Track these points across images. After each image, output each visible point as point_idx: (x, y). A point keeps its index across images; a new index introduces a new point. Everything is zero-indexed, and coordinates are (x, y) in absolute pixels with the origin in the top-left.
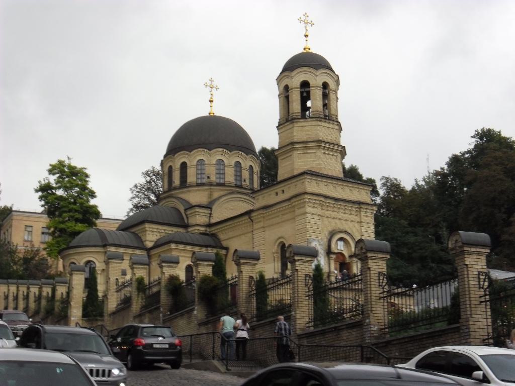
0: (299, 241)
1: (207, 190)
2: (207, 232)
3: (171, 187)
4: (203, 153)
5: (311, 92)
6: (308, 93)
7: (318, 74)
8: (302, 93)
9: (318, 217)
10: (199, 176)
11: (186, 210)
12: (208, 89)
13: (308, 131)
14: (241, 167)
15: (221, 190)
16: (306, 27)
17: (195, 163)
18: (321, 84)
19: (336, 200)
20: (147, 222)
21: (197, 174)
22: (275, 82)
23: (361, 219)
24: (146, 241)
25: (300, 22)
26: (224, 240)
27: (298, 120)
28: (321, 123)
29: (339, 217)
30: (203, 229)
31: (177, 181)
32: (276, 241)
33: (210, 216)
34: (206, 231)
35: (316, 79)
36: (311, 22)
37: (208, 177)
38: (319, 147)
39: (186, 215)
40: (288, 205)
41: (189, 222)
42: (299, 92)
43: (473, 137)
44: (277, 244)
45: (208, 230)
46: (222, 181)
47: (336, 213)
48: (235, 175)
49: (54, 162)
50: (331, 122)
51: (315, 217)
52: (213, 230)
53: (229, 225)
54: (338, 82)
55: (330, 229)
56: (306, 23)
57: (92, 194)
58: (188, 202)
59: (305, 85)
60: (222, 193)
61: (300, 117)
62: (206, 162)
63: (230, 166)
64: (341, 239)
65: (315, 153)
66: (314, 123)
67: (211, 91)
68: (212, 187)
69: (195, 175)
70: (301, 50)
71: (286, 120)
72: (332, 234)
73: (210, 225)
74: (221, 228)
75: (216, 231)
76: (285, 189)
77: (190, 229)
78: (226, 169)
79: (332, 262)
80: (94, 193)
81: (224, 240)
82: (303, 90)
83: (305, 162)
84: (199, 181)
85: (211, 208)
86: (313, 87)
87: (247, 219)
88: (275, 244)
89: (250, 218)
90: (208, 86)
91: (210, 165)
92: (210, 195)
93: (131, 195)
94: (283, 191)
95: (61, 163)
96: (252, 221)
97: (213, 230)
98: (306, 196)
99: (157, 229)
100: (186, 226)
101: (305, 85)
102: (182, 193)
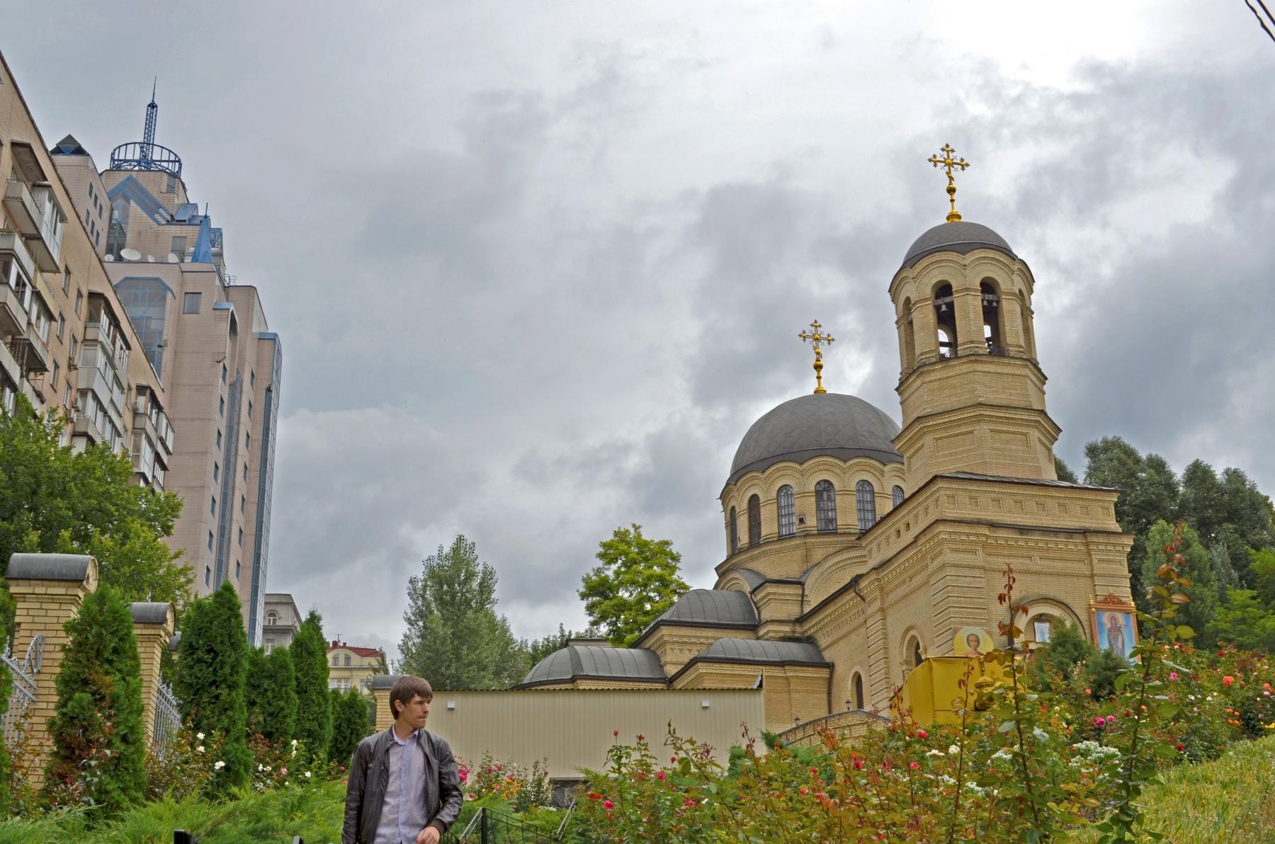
1: (798, 547)
3: (734, 551)
4: (789, 472)
7: (967, 262)
8: (938, 308)
9: (977, 573)
10: (784, 521)
13: (955, 387)
14: (872, 492)
15: (824, 544)
17: (774, 494)
19: (1022, 530)
22: (888, 296)
23: (1092, 569)
24: (666, 663)
27: (931, 368)
28: (979, 367)
29: (1033, 568)
30: (786, 629)
31: (744, 538)
34: (794, 632)
37: (801, 521)
38: (979, 419)
45: (798, 629)
47: (1028, 561)
48: (859, 510)
50: (1006, 361)
51: (967, 572)
52: (809, 628)
53: (833, 612)
54: (1029, 279)
56: (950, 165)
58: (758, 574)
59: (944, 290)
60: (831, 550)
62: (795, 490)
63: (845, 492)
64: (1040, 618)
65: (971, 432)
66: (965, 368)
67: (815, 348)
68: (809, 540)
71: (912, 371)
74: (819, 622)
76: (910, 518)
77: (761, 632)
82: (940, 301)
83: (950, 455)
84: (785, 531)
85: (802, 584)
86: (958, 291)
87: (852, 599)
88: (902, 643)
91: (803, 494)
92: (807, 558)
95: (621, 536)
98: (941, 528)
100: (752, 627)
101: (944, 290)
102: (752, 559)
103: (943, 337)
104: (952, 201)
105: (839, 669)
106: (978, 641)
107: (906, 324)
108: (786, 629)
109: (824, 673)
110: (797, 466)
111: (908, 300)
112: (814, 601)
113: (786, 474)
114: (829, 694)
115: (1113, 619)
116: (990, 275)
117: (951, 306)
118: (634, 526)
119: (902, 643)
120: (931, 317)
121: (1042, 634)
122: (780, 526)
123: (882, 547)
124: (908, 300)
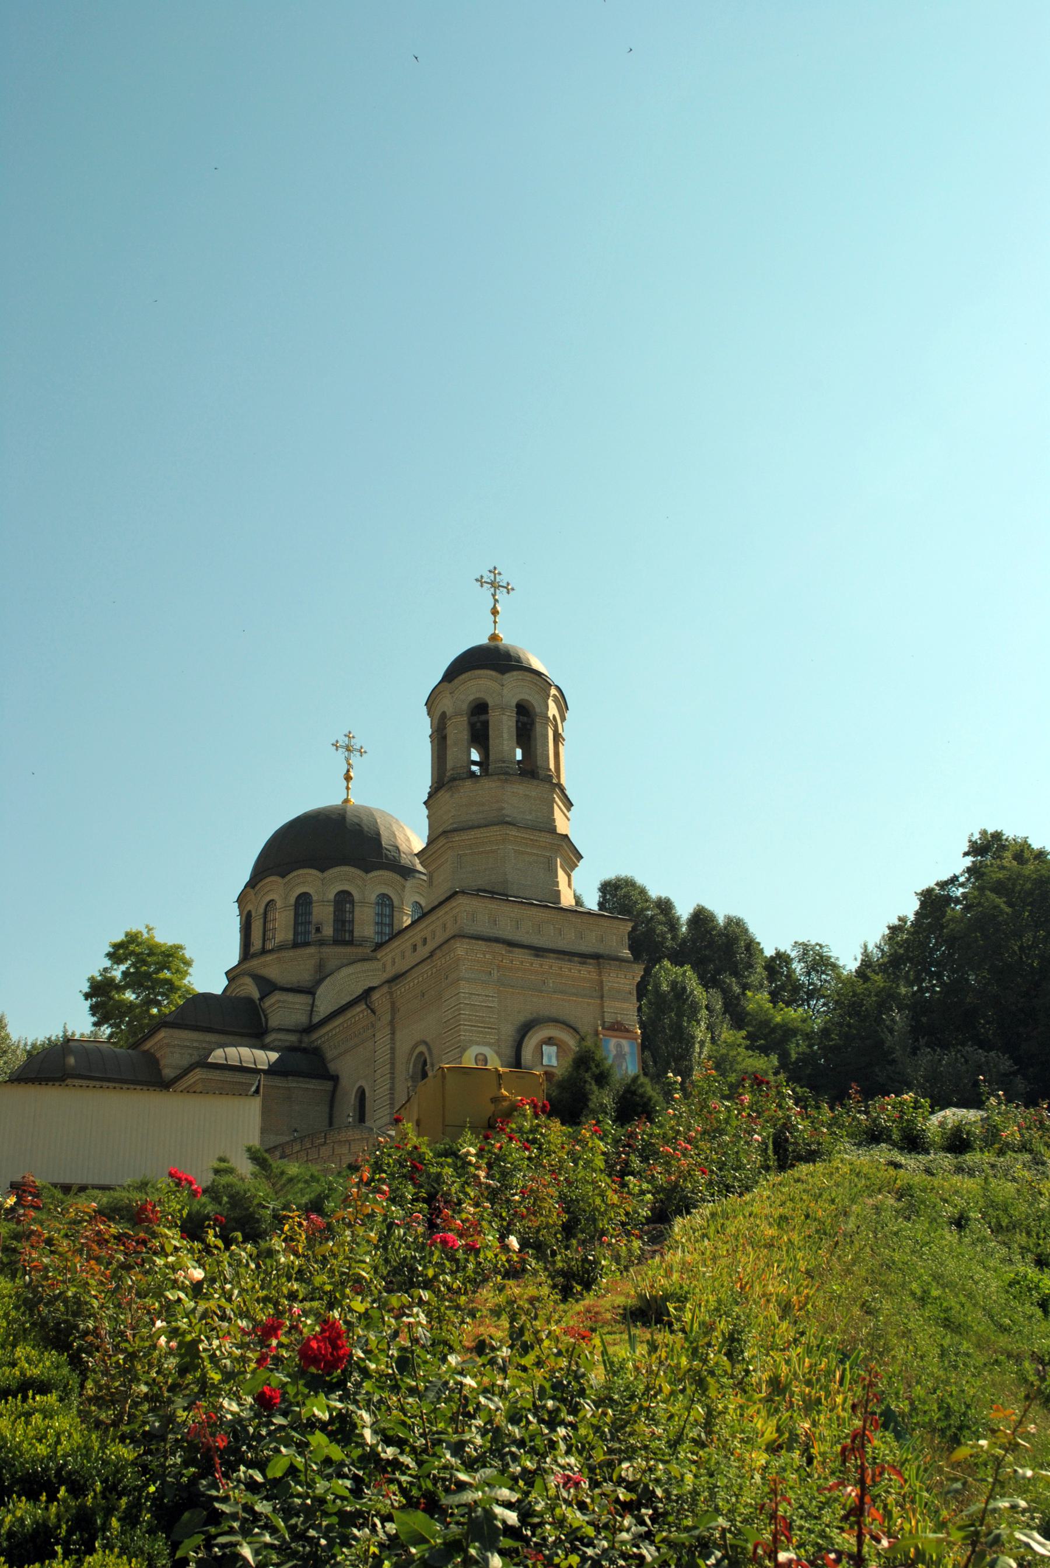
0: (448, 1047)
8: (472, 726)
12: (342, 753)
14: (392, 906)
16: (494, 595)
17: (292, 900)
18: (514, 703)
19: (539, 951)
20: (165, 1027)
21: (296, 924)
33: (312, 1011)
34: (300, 1042)
35: (505, 692)
37: (318, 930)
42: (466, 723)
43: (966, 854)
49: (120, 937)
55: (522, 1018)
64: (550, 1041)
67: (347, 760)
70: (484, 640)
72: (525, 1029)
78: (357, 909)
82: (475, 719)
87: (362, 1011)
89: (368, 1006)
90: (342, 747)
95: (132, 938)
96: (373, 1012)
101: (480, 708)
103: (475, 756)
104: (495, 622)
105: (345, 1082)
107: (440, 738)
108: (293, 1038)
109: (328, 1085)
111: (444, 714)
112: (324, 1008)
113: (307, 881)
114: (331, 1107)
115: (619, 1046)
116: (527, 697)
117: (486, 724)
118: (147, 927)
119: (409, 1060)
120: (465, 735)
121: (550, 1058)
122: (296, 934)
123: (395, 957)
124: (444, 714)
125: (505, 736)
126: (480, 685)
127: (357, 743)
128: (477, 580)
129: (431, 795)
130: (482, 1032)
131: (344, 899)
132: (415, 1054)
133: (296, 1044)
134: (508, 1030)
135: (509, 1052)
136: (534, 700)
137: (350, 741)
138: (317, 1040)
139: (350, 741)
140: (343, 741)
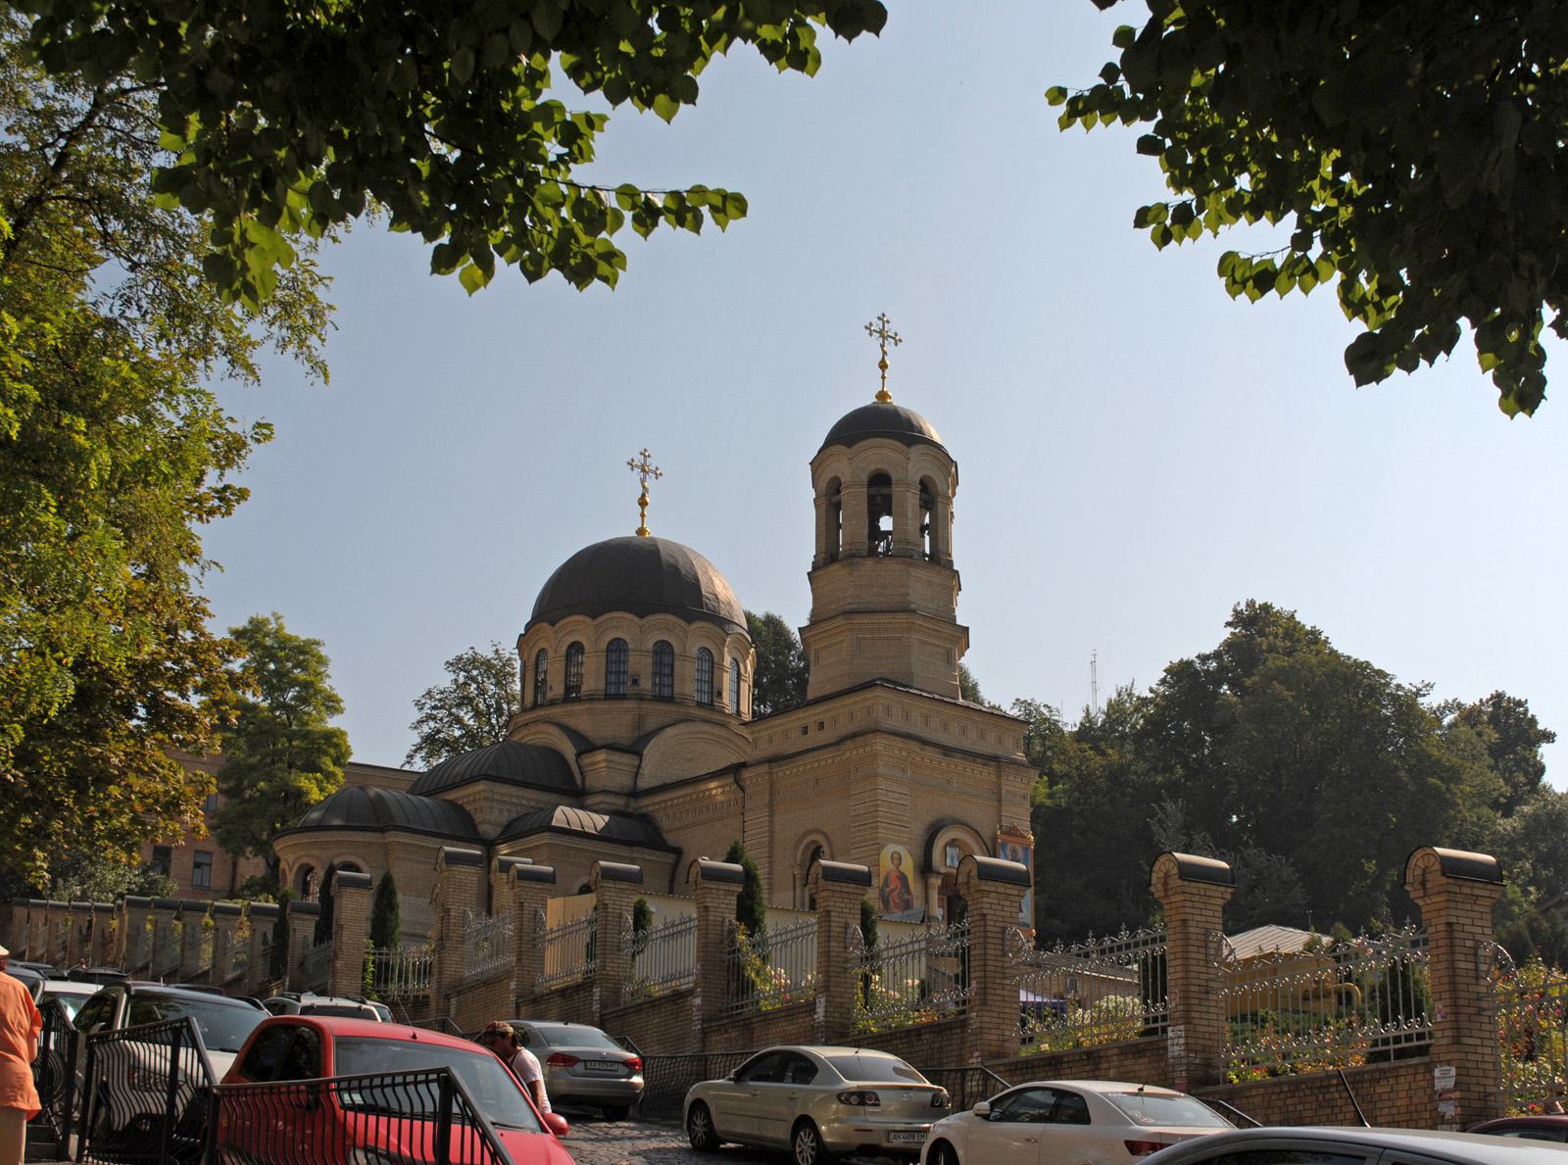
2: (630, 810)
5: (894, 498)
6: (888, 499)
8: (871, 499)
11: (578, 755)
12: (637, 474)
16: (882, 346)
17: (604, 646)
18: (918, 480)
19: (947, 751)
20: (488, 779)
25: (871, 335)
26: (667, 832)
32: (800, 841)
33: (637, 774)
36: (896, 334)
37: (635, 682)
39: (580, 767)
40: (833, 757)
41: (588, 783)
44: (802, 847)
46: (666, 692)
52: (647, 804)
55: (930, 818)
57: (332, 705)
61: (865, 553)
64: (953, 843)
65: (899, 639)
67: (643, 481)
69: (604, 676)
70: (868, 399)
71: (827, 558)
73: (635, 794)
75: (651, 808)
79: (934, 896)
80: (338, 701)
81: (667, 832)
82: (874, 491)
84: (612, 690)
85: (639, 755)
90: (637, 466)
93: (418, 716)
94: (821, 726)
96: (742, 789)
97: (647, 804)
99: (511, 796)
104: (883, 377)
106: (900, 859)
108: (619, 802)
109: (670, 858)
110: (636, 619)
113: (621, 625)
116: (929, 473)
118: (274, 614)
119: (797, 846)
125: (910, 514)
126: (879, 454)
127: (652, 463)
128: (866, 328)
129: (816, 567)
130: (894, 830)
131: (663, 651)
132: (805, 842)
133: (623, 809)
134: (918, 830)
135: (919, 851)
136: (937, 478)
137: (645, 460)
138: (647, 806)
139: (645, 460)
140: (639, 460)
